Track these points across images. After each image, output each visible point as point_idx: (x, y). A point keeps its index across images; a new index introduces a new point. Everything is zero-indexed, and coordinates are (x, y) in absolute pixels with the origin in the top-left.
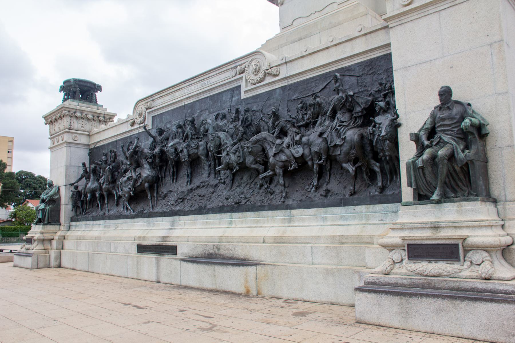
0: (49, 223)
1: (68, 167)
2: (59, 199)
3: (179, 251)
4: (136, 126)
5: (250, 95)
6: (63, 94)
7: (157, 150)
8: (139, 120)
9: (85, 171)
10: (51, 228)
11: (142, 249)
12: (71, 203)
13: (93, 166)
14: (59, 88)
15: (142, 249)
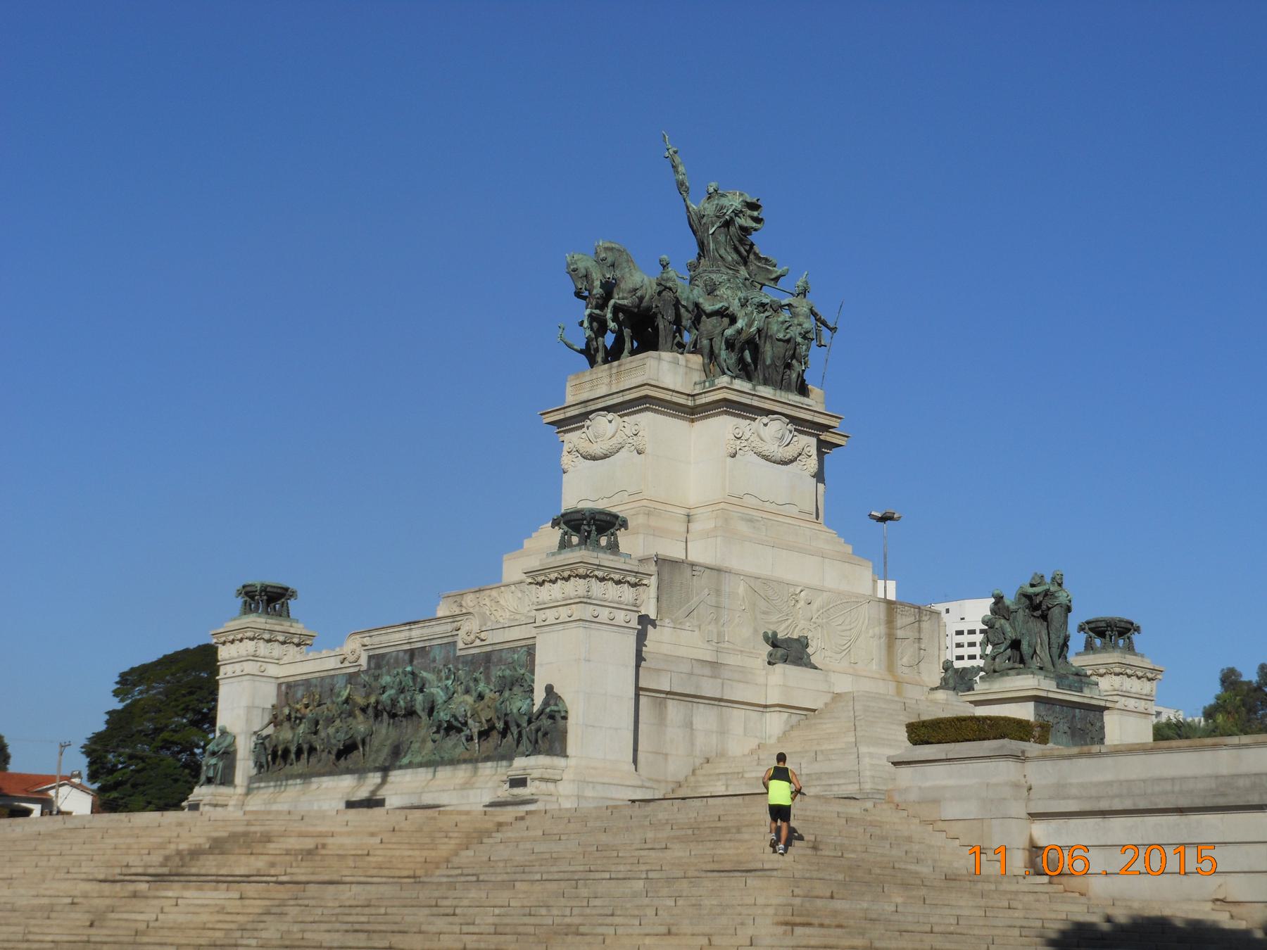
0: (222, 784)
1: (250, 708)
2: (235, 752)
3: (387, 803)
4: (346, 664)
5: (463, 653)
6: (240, 601)
7: (372, 700)
8: (352, 658)
9: (275, 717)
10: (223, 790)
11: (350, 805)
12: (252, 758)
13: (286, 711)
14: (234, 593)
15: (350, 805)
